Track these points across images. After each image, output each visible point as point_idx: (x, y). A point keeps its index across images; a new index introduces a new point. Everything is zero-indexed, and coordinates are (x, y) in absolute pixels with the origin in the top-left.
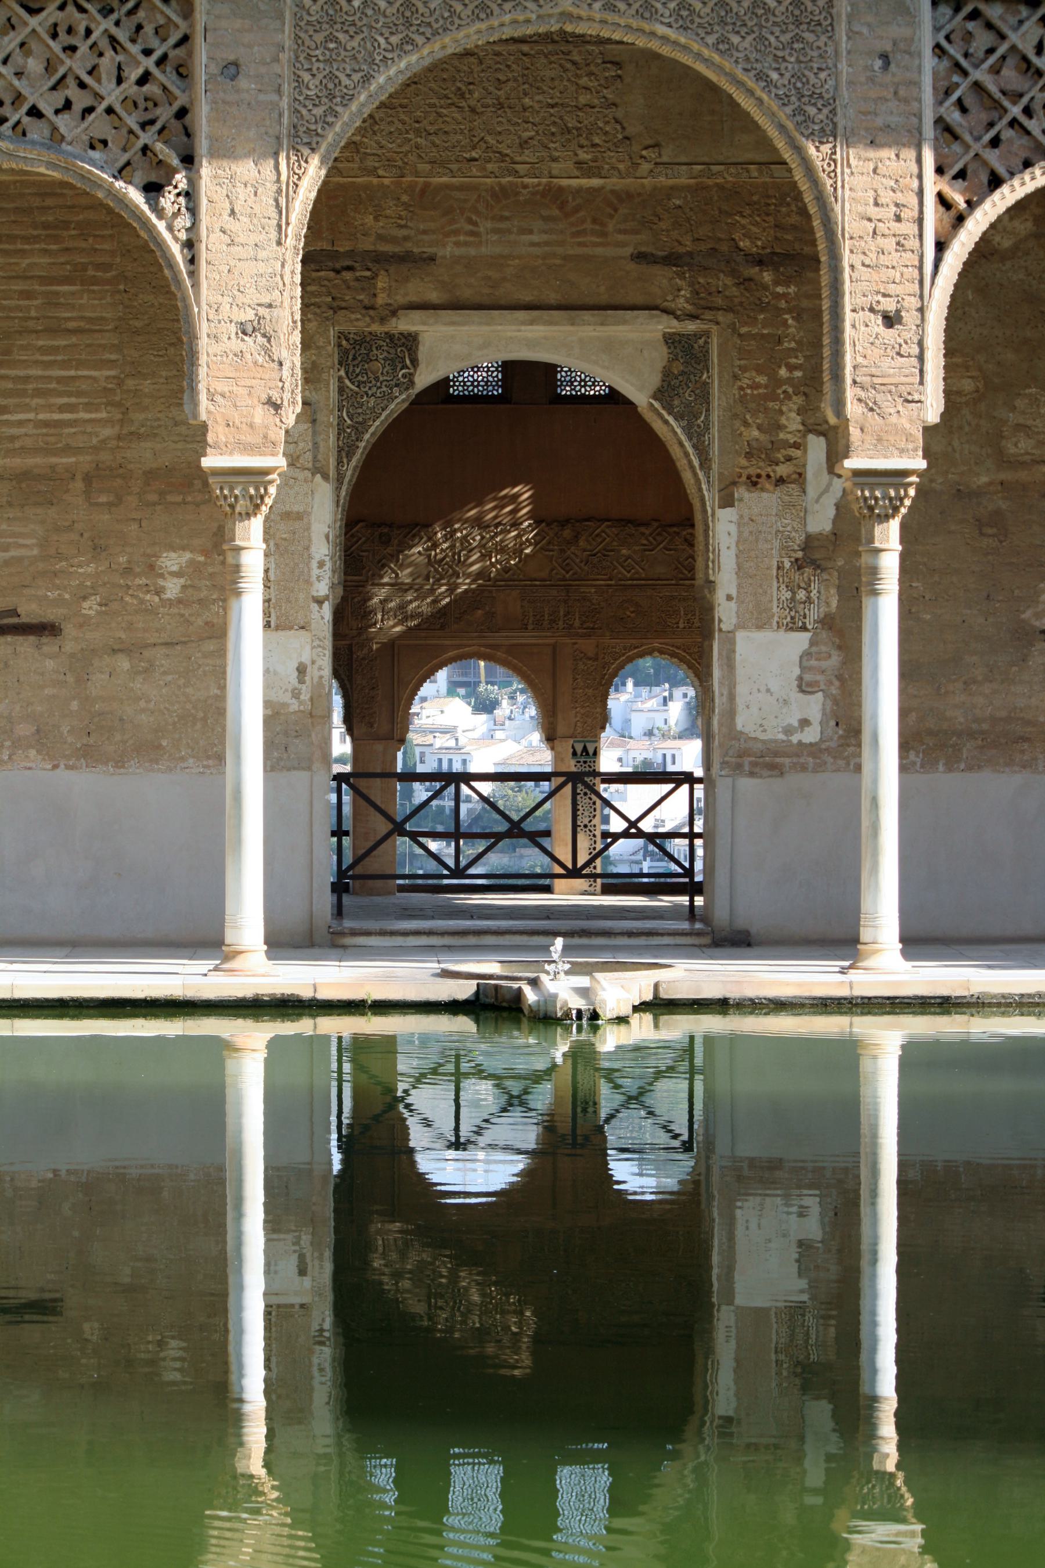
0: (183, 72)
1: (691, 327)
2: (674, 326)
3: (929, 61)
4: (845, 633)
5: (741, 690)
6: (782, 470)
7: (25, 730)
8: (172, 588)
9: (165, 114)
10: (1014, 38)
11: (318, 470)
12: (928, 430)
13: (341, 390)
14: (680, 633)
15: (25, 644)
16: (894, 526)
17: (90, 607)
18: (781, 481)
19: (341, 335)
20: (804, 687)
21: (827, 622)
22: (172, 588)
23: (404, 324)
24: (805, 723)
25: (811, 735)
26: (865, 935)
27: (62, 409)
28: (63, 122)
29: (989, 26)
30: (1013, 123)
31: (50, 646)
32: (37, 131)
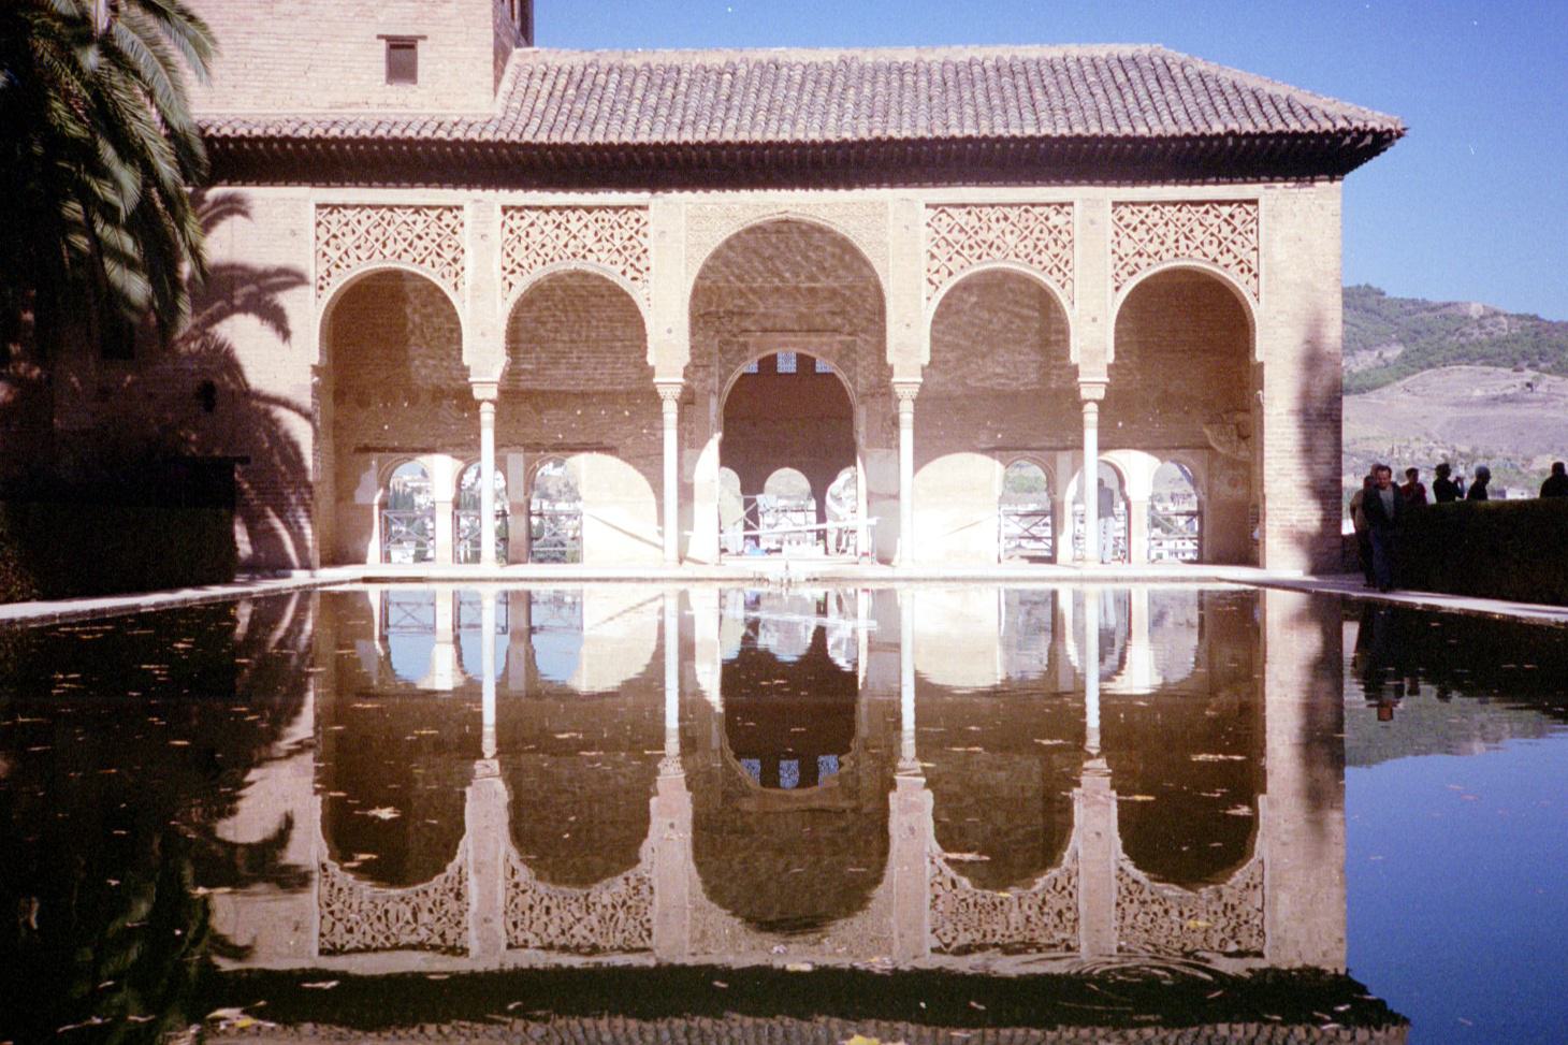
10: (957, 220)
17: (629, 441)
29: (949, 215)
30: (957, 252)
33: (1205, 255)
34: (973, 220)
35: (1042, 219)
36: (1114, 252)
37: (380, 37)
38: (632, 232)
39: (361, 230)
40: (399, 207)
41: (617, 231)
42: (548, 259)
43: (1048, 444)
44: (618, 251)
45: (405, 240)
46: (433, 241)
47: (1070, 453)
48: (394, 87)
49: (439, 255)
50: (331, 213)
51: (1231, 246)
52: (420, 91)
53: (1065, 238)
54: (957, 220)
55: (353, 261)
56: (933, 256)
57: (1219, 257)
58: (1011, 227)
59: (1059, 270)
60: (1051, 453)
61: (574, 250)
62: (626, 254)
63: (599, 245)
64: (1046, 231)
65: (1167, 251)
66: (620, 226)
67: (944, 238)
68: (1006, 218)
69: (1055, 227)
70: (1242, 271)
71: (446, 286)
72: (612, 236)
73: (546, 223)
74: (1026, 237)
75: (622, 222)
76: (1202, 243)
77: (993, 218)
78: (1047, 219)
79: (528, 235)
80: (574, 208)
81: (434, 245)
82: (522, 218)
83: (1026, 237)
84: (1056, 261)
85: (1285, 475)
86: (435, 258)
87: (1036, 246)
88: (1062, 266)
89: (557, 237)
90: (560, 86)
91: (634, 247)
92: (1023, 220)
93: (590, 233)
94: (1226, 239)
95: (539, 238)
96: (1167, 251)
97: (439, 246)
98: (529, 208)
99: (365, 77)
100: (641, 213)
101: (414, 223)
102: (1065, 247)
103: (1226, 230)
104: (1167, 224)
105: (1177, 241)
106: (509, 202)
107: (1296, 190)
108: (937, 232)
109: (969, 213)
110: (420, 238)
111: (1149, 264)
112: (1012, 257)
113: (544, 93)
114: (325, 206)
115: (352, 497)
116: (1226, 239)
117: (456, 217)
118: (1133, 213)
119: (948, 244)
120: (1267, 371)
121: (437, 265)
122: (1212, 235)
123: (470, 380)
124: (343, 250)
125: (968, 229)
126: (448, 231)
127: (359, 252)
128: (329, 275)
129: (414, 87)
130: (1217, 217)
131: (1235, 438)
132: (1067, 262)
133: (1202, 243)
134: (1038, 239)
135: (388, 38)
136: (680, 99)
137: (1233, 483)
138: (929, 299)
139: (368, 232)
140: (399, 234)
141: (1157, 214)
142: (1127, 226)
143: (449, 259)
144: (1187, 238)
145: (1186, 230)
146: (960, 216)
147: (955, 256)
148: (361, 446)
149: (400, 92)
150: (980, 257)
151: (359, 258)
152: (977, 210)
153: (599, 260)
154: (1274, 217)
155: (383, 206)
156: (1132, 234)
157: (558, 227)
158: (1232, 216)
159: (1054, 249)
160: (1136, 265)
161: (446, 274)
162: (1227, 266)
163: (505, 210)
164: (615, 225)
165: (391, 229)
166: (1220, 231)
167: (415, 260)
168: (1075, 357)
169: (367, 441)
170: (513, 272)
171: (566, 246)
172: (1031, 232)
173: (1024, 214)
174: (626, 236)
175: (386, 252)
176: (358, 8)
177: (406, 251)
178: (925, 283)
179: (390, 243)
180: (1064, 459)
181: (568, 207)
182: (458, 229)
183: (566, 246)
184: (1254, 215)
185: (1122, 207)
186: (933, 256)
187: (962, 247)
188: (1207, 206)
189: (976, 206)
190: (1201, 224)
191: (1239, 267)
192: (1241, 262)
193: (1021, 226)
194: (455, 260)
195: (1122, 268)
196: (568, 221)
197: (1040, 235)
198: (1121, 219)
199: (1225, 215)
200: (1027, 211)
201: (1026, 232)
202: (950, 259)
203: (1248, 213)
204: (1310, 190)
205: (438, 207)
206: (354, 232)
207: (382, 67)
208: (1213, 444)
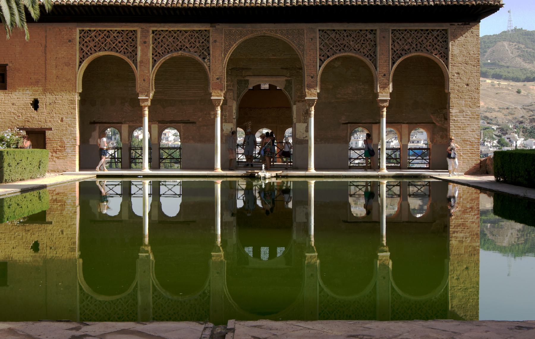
0: (208, 42)
1: (290, 79)
2: (287, 78)
3: (318, 39)
5: (297, 132)
7: (190, 137)
9: (206, 48)
10: (331, 36)
11: (234, 99)
12: (318, 93)
14: (290, 124)
15: (191, 125)
16: (313, 107)
17: (200, 120)
23: (247, 78)
26: (309, 167)
28: (191, 49)
32: (187, 50)
34: (337, 36)
35: (364, 36)
36: (392, 49)
38: (203, 40)
39: (97, 40)
42: (170, 51)
43: (369, 121)
46: (125, 44)
49: (126, 49)
50: (85, 33)
51: (437, 47)
53: (373, 43)
54: (331, 36)
55: (93, 51)
57: (433, 51)
58: (353, 39)
59: (371, 56)
60: (370, 125)
70: (442, 56)
72: (195, 41)
75: (199, 36)
77: (345, 35)
78: (366, 36)
82: (160, 35)
84: (370, 52)
93: (187, 41)
95: (167, 43)
103: (435, 41)
105: (416, 45)
107: (463, 26)
114: (83, 30)
115: (88, 141)
116: (435, 44)
117: (133, 34)
122: (430, 43)
125: (335, 39)
126: (131, 40)
127: (95, 48)
130: (433, 36)
131: (443, 119)
132: (374, 52)
134: (363, 44)
137: (442, 137)
138: (320, 66)
140: (111, 41)
141: (409, 35)
143: (131, 51)
146: (333, 35)
148: (92, 121)
150: (340, 51)
151: (95, 50)
158: (438, 36)
160: (401, 54)
165: (108, 40)
169: (94, 119)
170: (156, 56)
173: (358, 34)
174: (201, 42)
179: (108, 45)
180: (375, 127)
181: (178, 30)
185: (395, 32)
189: (338, 31)
190: (426, 39)
193: (356, 38)
196: (178, 36)
199: (435, 35)
202: (328, 51)
203: (444, 34)
204: (468, 26)
206: (93, 40)
208: (434, 122)
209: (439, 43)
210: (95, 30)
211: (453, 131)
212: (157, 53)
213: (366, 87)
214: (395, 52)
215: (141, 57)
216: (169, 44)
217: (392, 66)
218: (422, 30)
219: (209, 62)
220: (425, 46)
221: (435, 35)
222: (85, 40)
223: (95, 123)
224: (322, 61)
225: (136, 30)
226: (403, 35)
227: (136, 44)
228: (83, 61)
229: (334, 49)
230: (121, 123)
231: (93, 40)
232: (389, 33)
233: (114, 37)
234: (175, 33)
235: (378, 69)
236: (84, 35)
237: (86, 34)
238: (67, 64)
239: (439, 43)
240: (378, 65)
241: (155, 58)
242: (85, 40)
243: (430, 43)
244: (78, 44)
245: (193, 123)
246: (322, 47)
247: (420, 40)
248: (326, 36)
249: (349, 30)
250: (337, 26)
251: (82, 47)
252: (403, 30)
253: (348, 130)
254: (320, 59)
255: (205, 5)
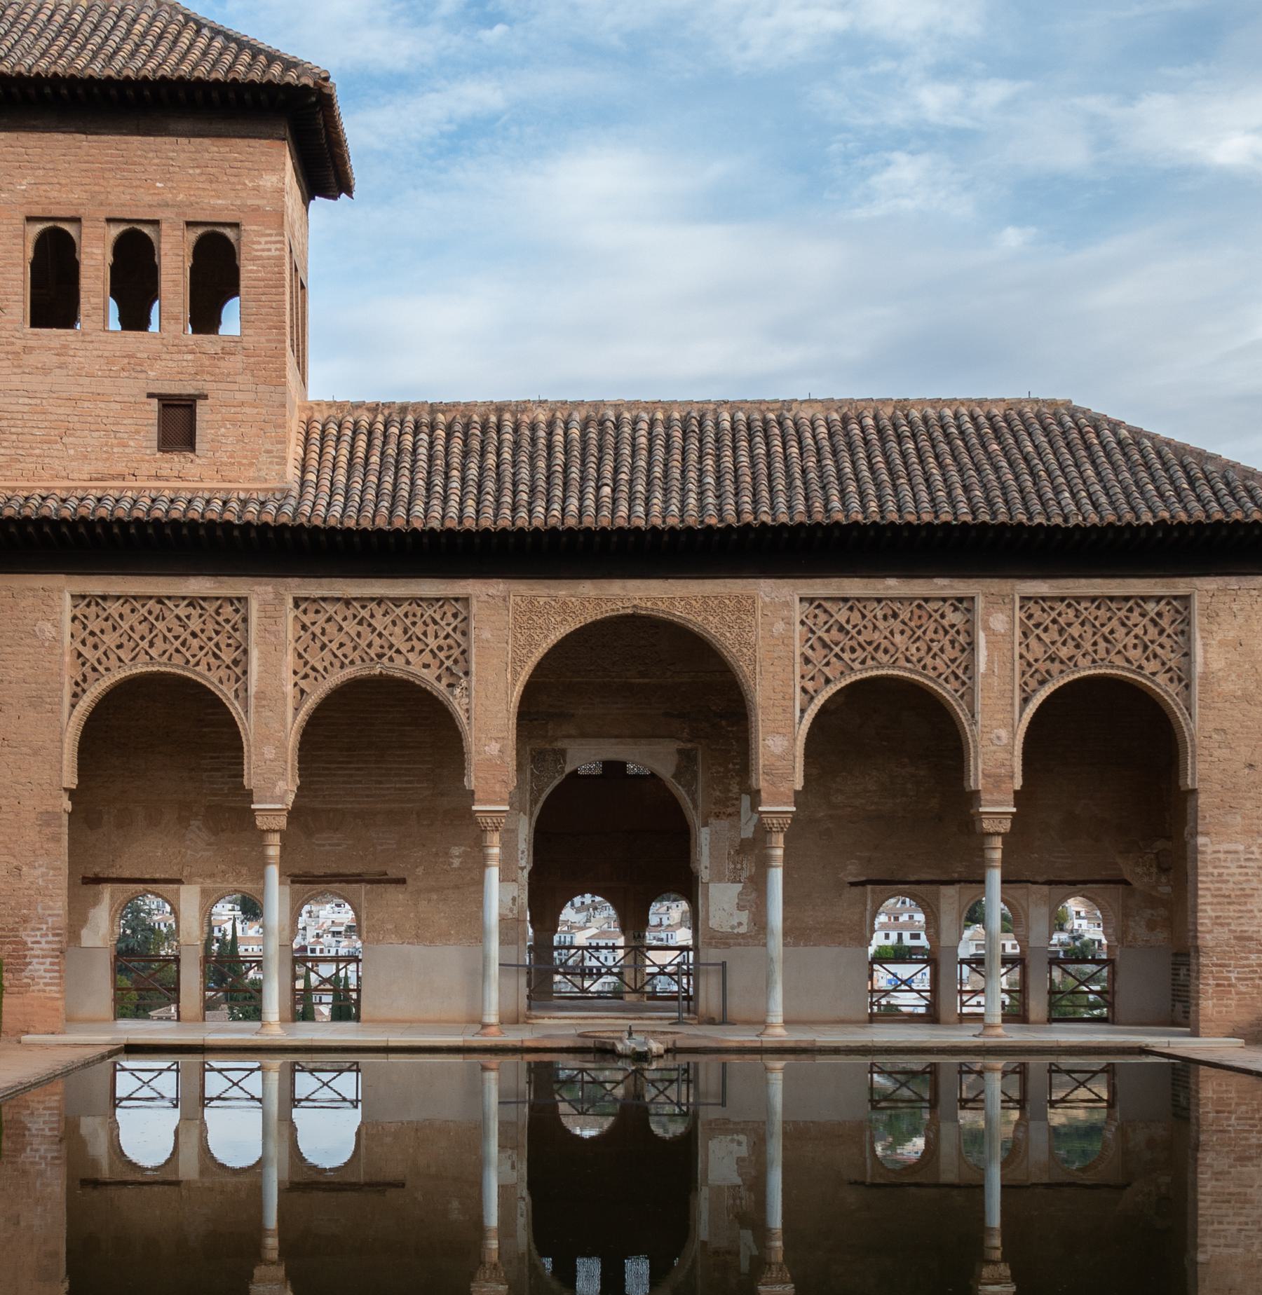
1: (689, 746)
2: (682, 745)
4: (758, 884)
5: (712, 909)
6: (730, 810)
8: (456, 863)
10: (836, 616)
11: (522, 810)
13: (532, 774)
16: (781, 836)
17: (420, 871)
18: (730, 815)
19: (532, 750)
20: (740, 907)
21: (751, 879)
22: (456, 863)
23: (559, 745)
24: (740, 924)
25: (743, 930)
27: (407, 782)
29: (826, 611)
31: (400, 888)
33: (1128, 661)
35: (937, 616)
36: (1021, 657)
37: (150, 396)
38: (449, 630)
39: (125, 626)
40: (169, 598)
41: (431, 629)
42: (347, 661)
44: (432, 651)
45: (176, 638)
46: (210, 639)
47: (957, 886)
48: (168, 456)
49: (215, 655)
50: (88, 605)
52: (198, 461)
53: (962, 639)
54: (836, 616)
55: (113, 662)
56: (807, 660)
57: (1144, 663)
58: (902, 627)
59: (957, 677)
61: (380, 650)
62: (442, 655)
63: (409, 645)
64: (941, 632)
65: (1084, 655)
66: (435, 622)
67: (820, 638)
68: (895, 616)
69: (953, 626)
70: (1171, 680)
71: (226, 693)
72: (425, 634)
73: (345, 619)
74: (919, 638)
75: (438, 618)
76: (1125, 647)
77: (880, 614)
78: (943, 616)
79: (323, 633)
80: (380, 601)
81: (211, 644)
82: (317, 612)
83: (919, 638)
84: (953, 667)
85: (1222, 925)
86: (212, 660)
87: (930, 649)
88: (960, 672)
89: (359, 635)
90: (361, 453)
91: (450, 648)
92: (916, 617)
93: (398, 630)
94: (1152, 642)
96: (1084, 655)
97: (217, 645)
98: (324, 599)
99: (132, 443)
100: (459, 606)
101: (188, 617)
102: (963, 650)
103: (1153, 632)
104: (1082, 624)
105: (1095, 644)
106: (303, 593)
108: (813, 632)
109: (851, 609)
110: (194, 635)
111: (1062, 672)
112: (902, 662)
113: (343, 461)
114: (84, 597)
116: (1152, 642)
117: (237, 611)
118: (1043, 610)
119: (825, 645)
120: (1202, 799)
121: (214, 669)
122: (1136, 637)
123: (253, 806)
124: (102, 649)
125: (849, 627)
126: (228, 627)
127: (121, 653)
128: (85, 680)
129: (191, 456)
130: (1143, 615)
133: (1125, 647)
134: (932, 641)
135: (160, 397)
136: (508, 470)
138: (803, 711)
139: (132, 628)
141: (1071, 613)
142: (1037, 626)
143: (228, 661)
144: (1107, 640)
145: (1106, 630)
147: (834, 660)
149: (177, 461)
150: (863, 662)
151: (120, 660)
152: (860, 606)
153: (408, 662)
154: (1208, 617)
155: (150, 598)
156: (1043, 636)
157: (360, 623)
159: (950, 653)
160: (1048, 672)
161: (225, 679)
162: (1154, 674)
163: (297, 602)
164: (429, 621)
165: (160, 625)
166: (1145, 633)
167: (188, 662)
168: (977, 779)
170: (306, 676)
171: (370, 645)
172: (924, 633)
174: (442, 635)
175: (153, 652)
176: (126, 361)
177: (177, 651)
178: (798, 690)
179: (159, 642)
181: (373, 599)
182: (240, 626)
183: (370, 645)
184: (1185, 613)
185: (1031, 604)
186: (807, 660)
187: (843, 650)
188: (1131, 603)
189: (858, 600)
190: (1124, 625)
191: (1169, 675)
192: (1170, 669)
194: (236, 662)
195: (1032, 676)
196: (372, 616)
197: (934, 636)
198: (1030, 617)
200: (919, 606)
201: (919, 633)
202: (827, 664)
205: (217, 598)
206: (114, 628)
207: (152, 433)
209: (1163, 639)
210: (119, 598)
211: (1208, 908)
212: (307, 670)
213: (922, 773)
214: (1029, 665)
215: (260, 679)
216: (345, 640)
217: (1022, 711)
218: (1112, 599)
219: (468, 696)
220: (1120, 646)
221: (1152, 614)
222: (90, 627)
223: (98, 880)
224: (809, 696)
225: (246, 599)
226: (1054, 614)
227: (246, 639)
228: (84, 691)
229: (846, 656)
230: (179, 882)
231: (114, 628)
232: (1013, 609)
233: (178, 617)
234: (363, 607)
235: (979, 717)
236: (87, 611)
237: (93, 608)
238: (35, 702)
239: (1163, 639)
240: (978, 706)
241: (303, 684)
242: (90, 627)
243: (1136, 637)
244: (68, 639)
245: (402, 881)
246: (810, 653)
247: (1106, 630)
248: (822, 617)
249: (891, 599)
250: (854, 587)
251: (81, 648)
252: (1053, 599)
253: (865, 905)
254: (804, 690)
255: (460, 522)
